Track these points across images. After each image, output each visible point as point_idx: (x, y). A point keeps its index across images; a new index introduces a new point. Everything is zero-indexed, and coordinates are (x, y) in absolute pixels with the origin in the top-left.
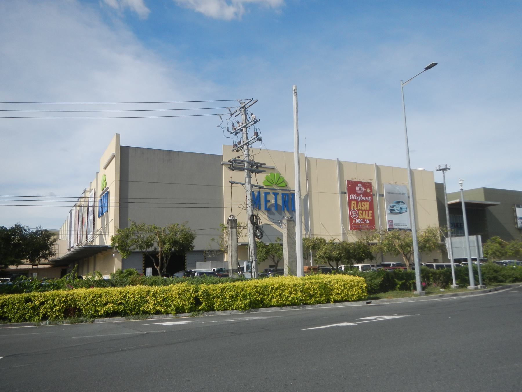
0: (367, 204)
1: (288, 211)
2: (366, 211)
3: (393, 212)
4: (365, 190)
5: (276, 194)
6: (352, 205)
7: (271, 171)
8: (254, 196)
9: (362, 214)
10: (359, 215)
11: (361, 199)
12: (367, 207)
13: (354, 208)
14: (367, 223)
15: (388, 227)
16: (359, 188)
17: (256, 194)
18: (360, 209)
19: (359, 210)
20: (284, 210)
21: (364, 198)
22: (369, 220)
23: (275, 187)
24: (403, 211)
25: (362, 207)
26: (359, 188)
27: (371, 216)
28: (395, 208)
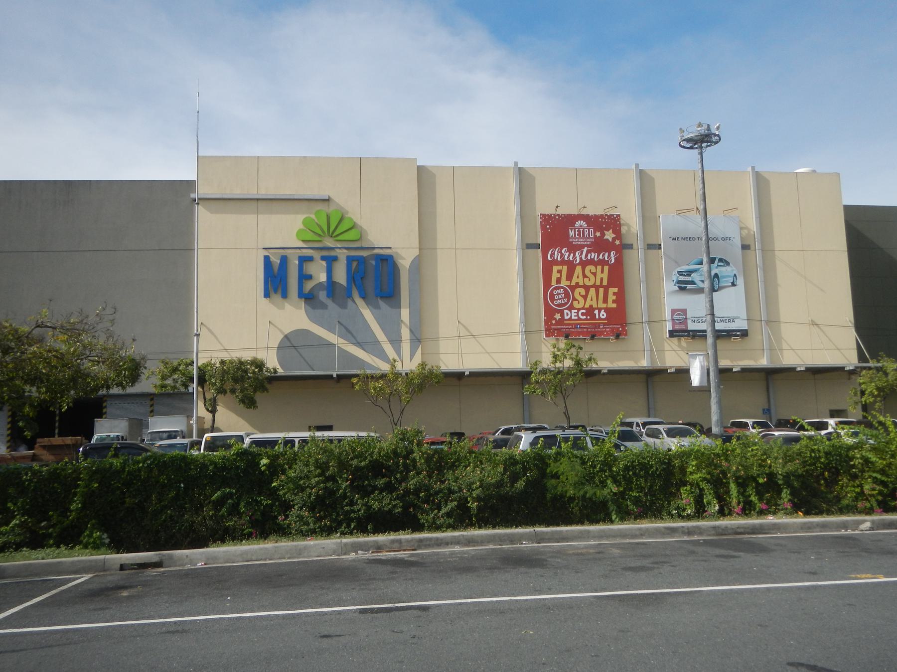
0: (602, 272)
1: (364, 297)
2: (597, 288)
3: (689, 287)
4: (598, 234)
5: (331, 261)
6: (555, 275)
7: (320, 206)
8: (272, 266)
9: (585, 297)
10: (576, 300)
11: (583, 259)
12: (602, 279)
13: (559, 281)
14: (600, 319)
15: (669, 326)
16: (579, 231)
17: (276, 260)
18: (577, 284)
19: (577, 285)
20: (350, 296)
21: (593, 256)
22: (607, 310)
23: (329, 243)
24: (722, 284)
25: (586, 280)
26: (579, 233)
27: (614, 302)
28: (695, 277)
